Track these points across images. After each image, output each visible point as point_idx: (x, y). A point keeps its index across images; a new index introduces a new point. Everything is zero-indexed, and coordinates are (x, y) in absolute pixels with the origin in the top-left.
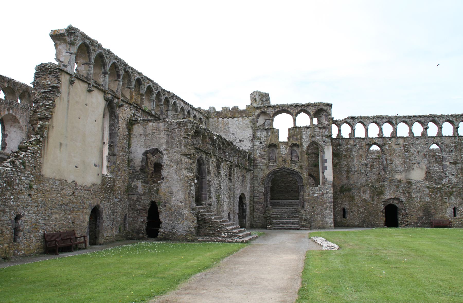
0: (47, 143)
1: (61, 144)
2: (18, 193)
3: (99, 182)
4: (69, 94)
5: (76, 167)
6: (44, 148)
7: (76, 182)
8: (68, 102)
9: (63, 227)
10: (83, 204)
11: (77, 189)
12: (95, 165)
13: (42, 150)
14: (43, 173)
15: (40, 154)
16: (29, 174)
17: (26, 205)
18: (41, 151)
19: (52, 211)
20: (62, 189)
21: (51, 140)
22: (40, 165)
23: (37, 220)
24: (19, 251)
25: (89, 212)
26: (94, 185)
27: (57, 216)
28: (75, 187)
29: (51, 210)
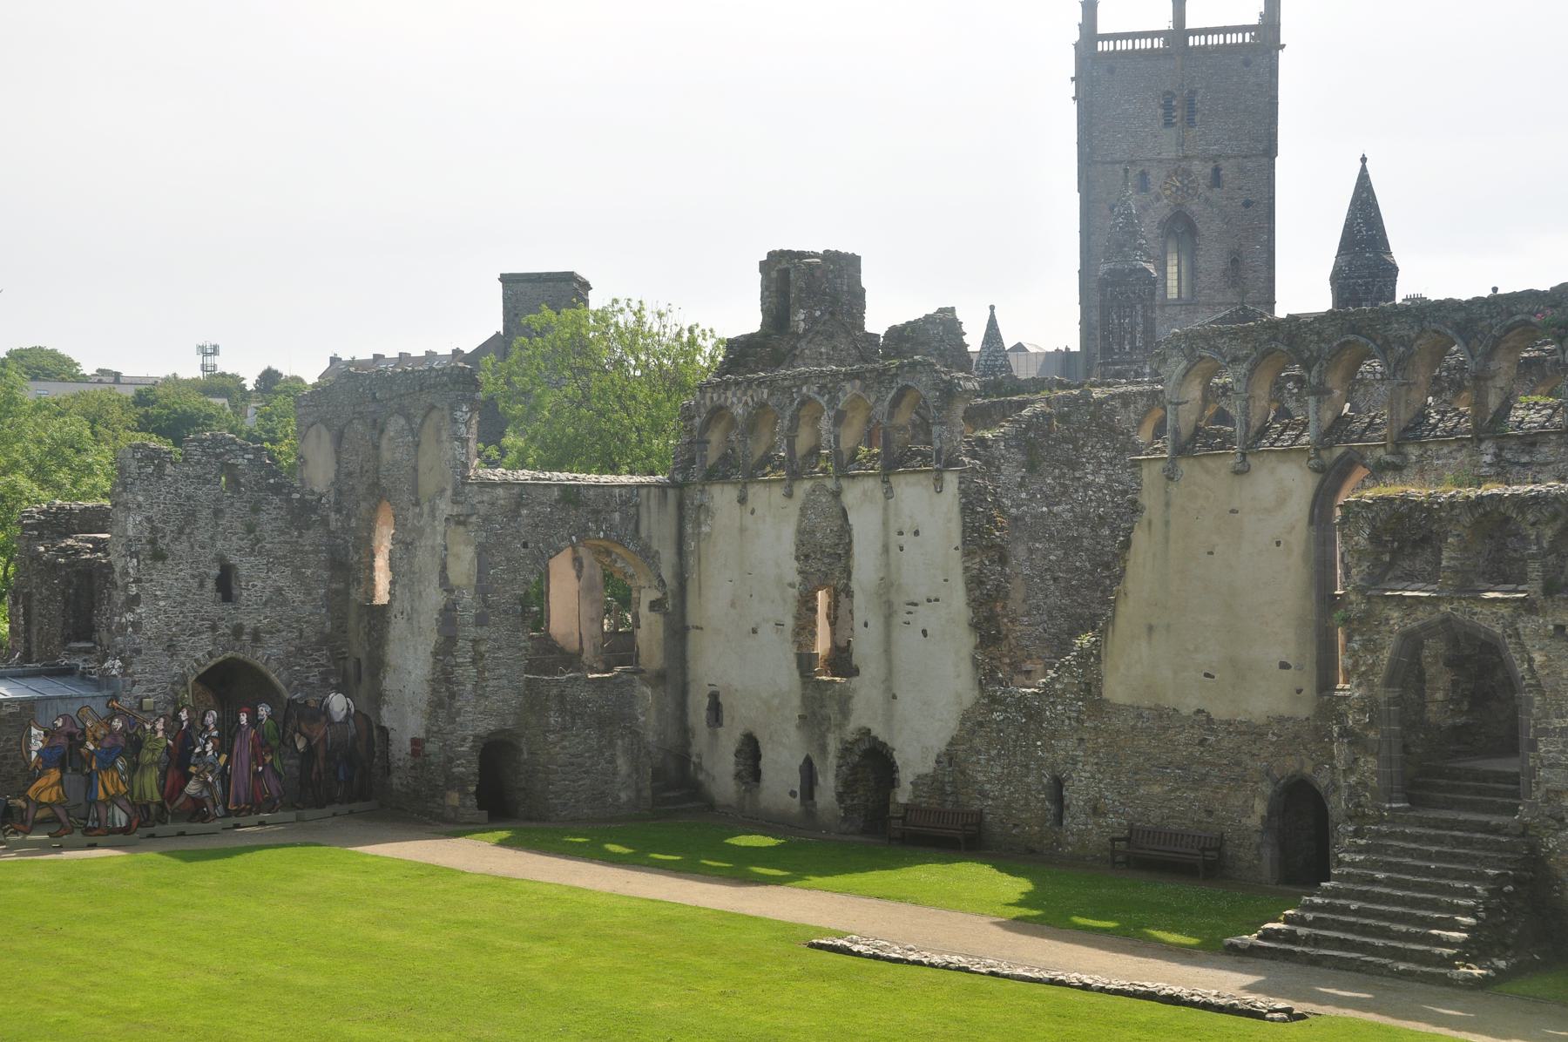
0: (1113, 631)
1: (1151, 628)
2: (1053, 735)
3: (1304, 710)
4: (1167, 505)
5: (1207, 675)
6: (1106, 642)
7: (1208, 716)
8: (1167, 523)
9: (1173, 817)
10: (1237, 769)
11: (1213, 731)
12: (1284, 666)
13: (1103, 649)
14: (1106, 695)
15: (1098, 657)
16: (1074, 699)
17: (1073, 759)
18: (1099, 651)
19: (1138, 777)
20: (1165, 729)
21: (1121, 622)
22: (1100, 680)
23: (1100, 791)
24: (1059, 845)
25: (1267, 788)
26: (1281, 720)
27: (1157, 789)
28: (1208, 723)
29: (1136, 773)
